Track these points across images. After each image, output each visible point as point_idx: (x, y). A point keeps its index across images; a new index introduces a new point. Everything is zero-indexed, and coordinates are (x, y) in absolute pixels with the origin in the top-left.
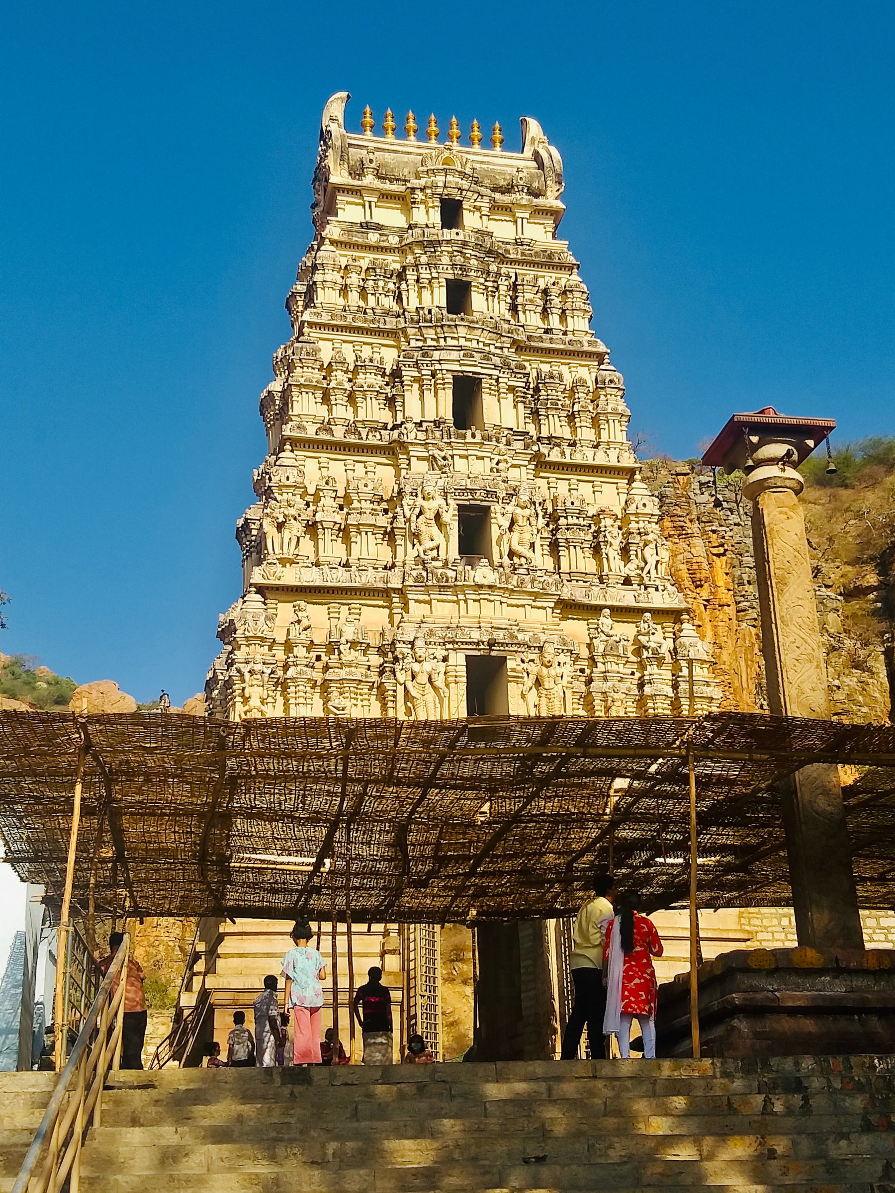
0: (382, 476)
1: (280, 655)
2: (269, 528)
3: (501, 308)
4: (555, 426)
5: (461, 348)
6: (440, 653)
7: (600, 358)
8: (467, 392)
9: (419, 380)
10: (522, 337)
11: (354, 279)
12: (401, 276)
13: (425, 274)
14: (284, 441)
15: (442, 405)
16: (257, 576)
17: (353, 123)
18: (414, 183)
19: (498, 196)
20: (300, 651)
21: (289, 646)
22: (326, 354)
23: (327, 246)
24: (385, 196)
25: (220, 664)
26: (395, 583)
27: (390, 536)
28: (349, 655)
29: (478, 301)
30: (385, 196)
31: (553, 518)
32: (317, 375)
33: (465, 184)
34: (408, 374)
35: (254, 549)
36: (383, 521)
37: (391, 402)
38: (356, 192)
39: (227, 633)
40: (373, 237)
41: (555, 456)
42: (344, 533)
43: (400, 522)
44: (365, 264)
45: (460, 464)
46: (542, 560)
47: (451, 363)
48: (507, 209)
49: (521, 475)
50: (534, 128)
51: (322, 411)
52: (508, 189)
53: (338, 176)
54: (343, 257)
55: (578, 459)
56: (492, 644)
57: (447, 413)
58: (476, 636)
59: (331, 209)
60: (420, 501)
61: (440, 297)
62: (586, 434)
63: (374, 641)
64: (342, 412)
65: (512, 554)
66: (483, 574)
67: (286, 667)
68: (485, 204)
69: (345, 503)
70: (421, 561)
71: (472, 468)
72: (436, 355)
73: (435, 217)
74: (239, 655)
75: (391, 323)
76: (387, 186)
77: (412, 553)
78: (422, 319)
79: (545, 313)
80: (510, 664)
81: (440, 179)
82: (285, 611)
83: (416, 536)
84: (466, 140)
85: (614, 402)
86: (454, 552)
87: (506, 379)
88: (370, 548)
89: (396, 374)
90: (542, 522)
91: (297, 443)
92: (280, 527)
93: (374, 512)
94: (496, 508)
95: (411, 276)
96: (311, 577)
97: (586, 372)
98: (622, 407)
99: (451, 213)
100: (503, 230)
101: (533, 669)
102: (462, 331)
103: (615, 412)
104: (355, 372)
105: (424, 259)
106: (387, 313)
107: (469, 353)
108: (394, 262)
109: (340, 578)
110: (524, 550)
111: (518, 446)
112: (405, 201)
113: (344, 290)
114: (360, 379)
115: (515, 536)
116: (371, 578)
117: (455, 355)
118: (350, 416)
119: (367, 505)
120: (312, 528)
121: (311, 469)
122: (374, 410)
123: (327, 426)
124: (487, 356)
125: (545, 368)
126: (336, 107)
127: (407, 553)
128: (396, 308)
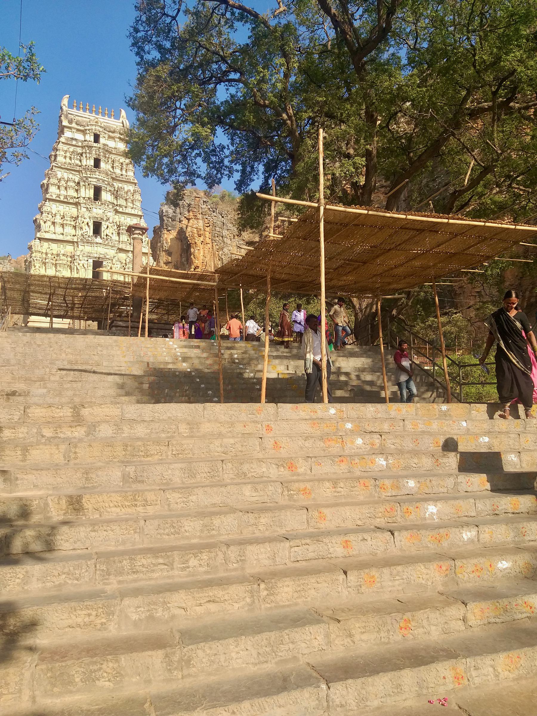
0: (74, 211)
1: (44, 256)
2: (42, 223)
3: (109, 167)
4: (122, 202)
5: (96, 178)
6: (86, 259)
7: (135, 184)
8: (97, 191)
9: (85, 186)
10: (114, 176)
11: (68, 155)
12: (82, 155)
13: (88, 155)
14: (47, 199)
15: (91, 193)
16: (38, 235)
17: (71, 106)
18: (87, 128)
19: (110, 134)
20: (49, 255)
21: (46, 254)
22: (59, 175)
23: (61, 144)
24: (78, 130)
25: (28, 256)
26: (75, 240)
27: (75, 227)
28: (62, 257)
29: (102, 165)
30: (78, 130)
31: (119, 226)
32: (56, 182)
33: (101, 130)
34: (82, 183)
35: (38, 228)
36: (73, 223)
37: (77, 191)
38: (70, 128)
39: (30, 248)
40: (74, 143)
41: (121, 210)
42: (63, 225)
43: (77, 224)
44: (71, 150)
45: (94, 210)
46: (115, 237)
47: (94, 182)
48: (113, 138)
49: (111, 214)
50: (123, 113)
51: (57, 191)
52: (114, 132)
53: (65, 123)
54: (66, 148)
55: (127, 211)
56: (99, 258)
57: (92, 195)
58: (96, 255)
59: (62, 132)
60: (83, 219)
61: (92, 163)
62: (130, 204)
63: (69, 254)
64: (63, 192)
65: (107, 235)
66: (98, 240)
67: (46, 259)
68: (106, 136)
69: (63, 217)
70: (82, 235)
71: (98, 211)
72: (90, 179)
73: (92, 139)
74: (33, 255)
75: (78, 168)
76: (79, 127)
77: (80, 233)
78: (86, 169)
79: (121, 169)
80: (104, 263)
81: (94, 127)
82: (46, 245)
83: (81, 228)
84: (103, 115)
85: (138, 197)
86: (91, 233)
87: (109, 188)
88: (69, 230)
89: (79, 183)
90: (116, 227)
91: (50, 200)
92: (45, 222)
93: (71, 221)
94: (103, 223)
95: (84, 155)
96: (54, 237)
97: (131, 188)
98: (140, 198)
99: (97, 138)
100: (111, 144)
101: (110, 265)
102: (97, 173)
103: (138, 200)
104: (67, 181)
105: (88, 151)
106: (77, 165)
107: (99, 180)
108: (79, 150)
109: (61, 237)
110: (110, 235)
111: (111, 206)
112: (84, 132)
113: (65, 157)
114: (69, 183)
115: (108, 231)
116: (69, 238)
117: (95, 180)
118: (65, 194)
119: (69, 219)
120: (54, 223)
121: (54, 207)
122: (72, 193)
123: (59, 196)
124: (104, 181)
125: (120, 185)
126: (65, 101)
127: (79, 232)
128: (80, 164)
